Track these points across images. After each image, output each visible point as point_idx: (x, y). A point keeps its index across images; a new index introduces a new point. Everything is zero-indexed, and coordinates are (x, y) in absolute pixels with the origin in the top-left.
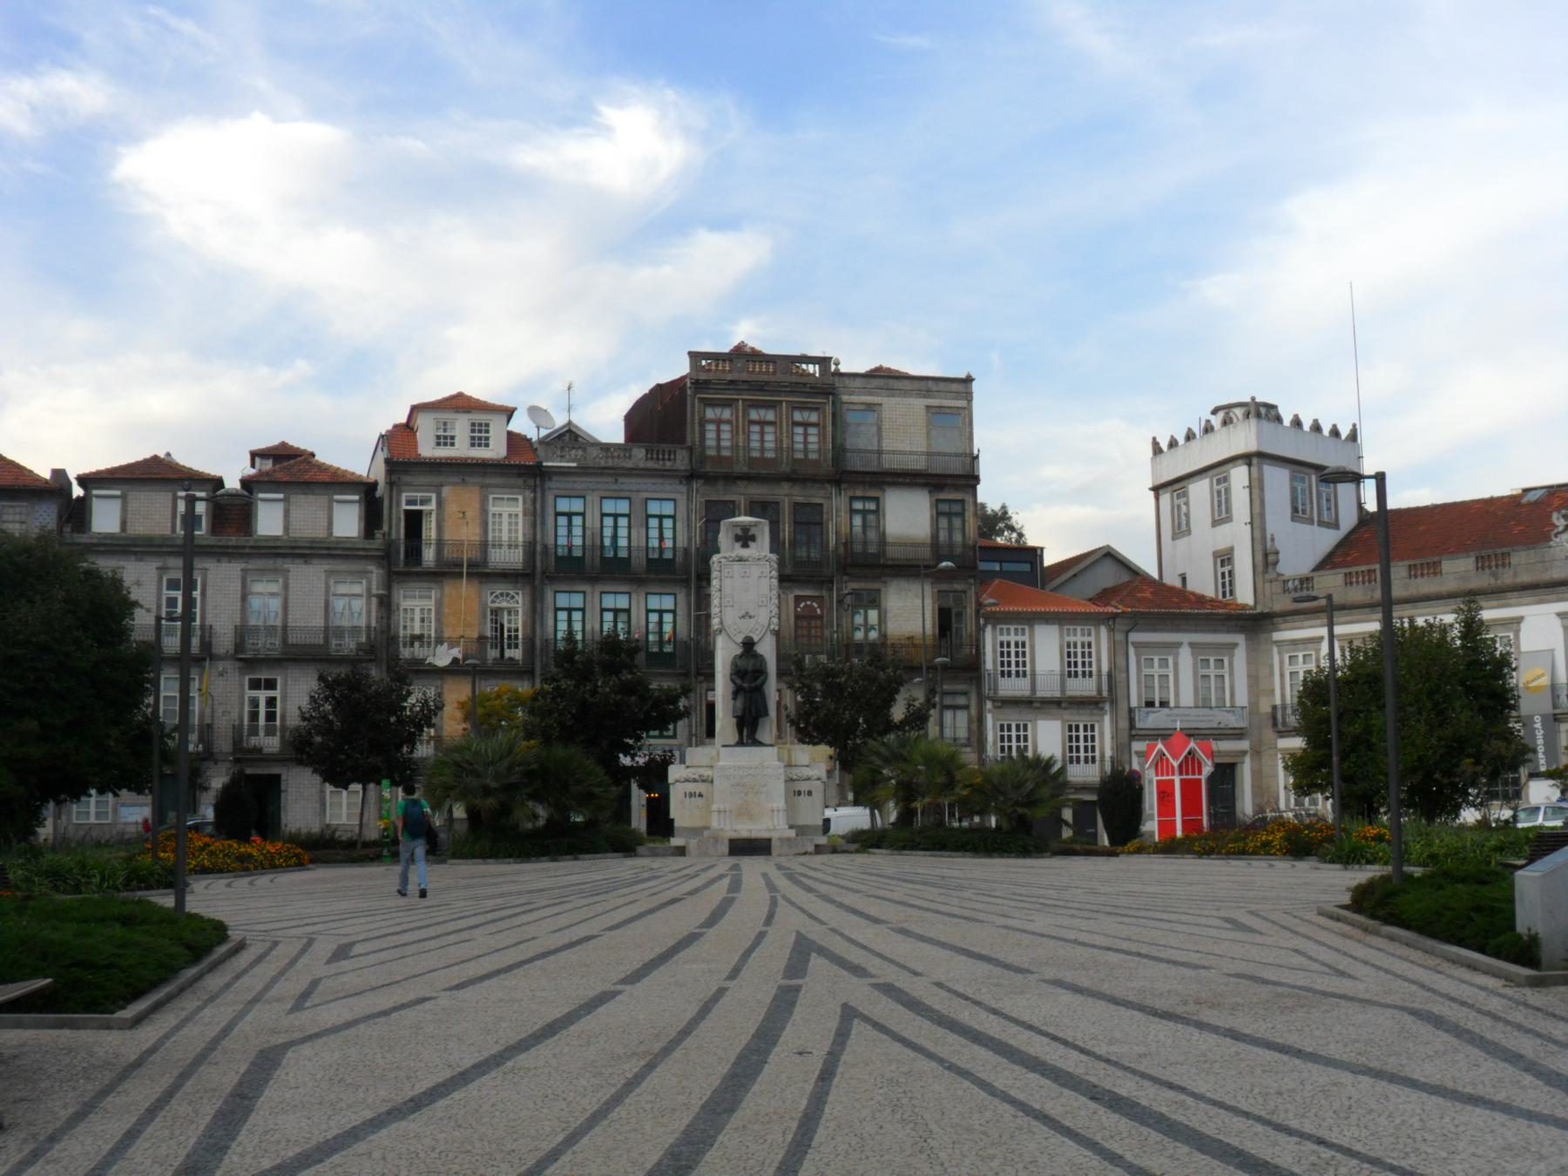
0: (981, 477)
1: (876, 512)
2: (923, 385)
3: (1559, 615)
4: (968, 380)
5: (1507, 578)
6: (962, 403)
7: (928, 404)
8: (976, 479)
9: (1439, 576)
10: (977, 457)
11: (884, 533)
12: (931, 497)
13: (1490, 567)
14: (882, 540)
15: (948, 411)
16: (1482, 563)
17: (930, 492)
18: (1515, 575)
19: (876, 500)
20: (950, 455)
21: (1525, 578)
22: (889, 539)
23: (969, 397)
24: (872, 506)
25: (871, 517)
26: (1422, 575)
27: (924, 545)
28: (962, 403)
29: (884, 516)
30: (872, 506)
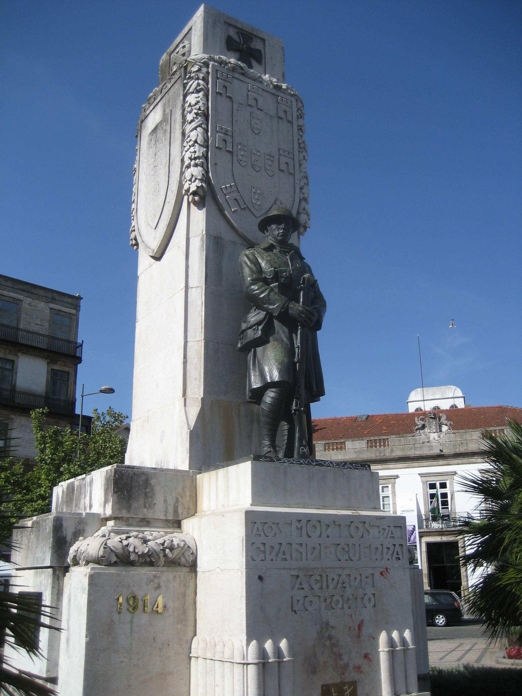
0: (83, 359)
1: (12, 370)
2: (49, 295)
3: (421, 475)
4: (79, 298)
5: (387, 453)
6: (73, 311)
7: (52, 307)
8: (79, 360)
9: (343, 450)
10: (81, 346)
11: (15, 386)
12: (48, 366)
13: (376, 447)
14: (13, 389)
15: (64, 314)
16: (371, 444)
17: (48, 363)
18: (392, 451)
19: (13, 362)
20: (62, 340)
21: (399, 453)
22: (18, 389)
23: (77, 307)
24: (8, 366)
25: (7, 373)
26: (333, 449)
27: (40, 396)
28: (73, 311)
29: (16, 373)
30: (8, 366)
